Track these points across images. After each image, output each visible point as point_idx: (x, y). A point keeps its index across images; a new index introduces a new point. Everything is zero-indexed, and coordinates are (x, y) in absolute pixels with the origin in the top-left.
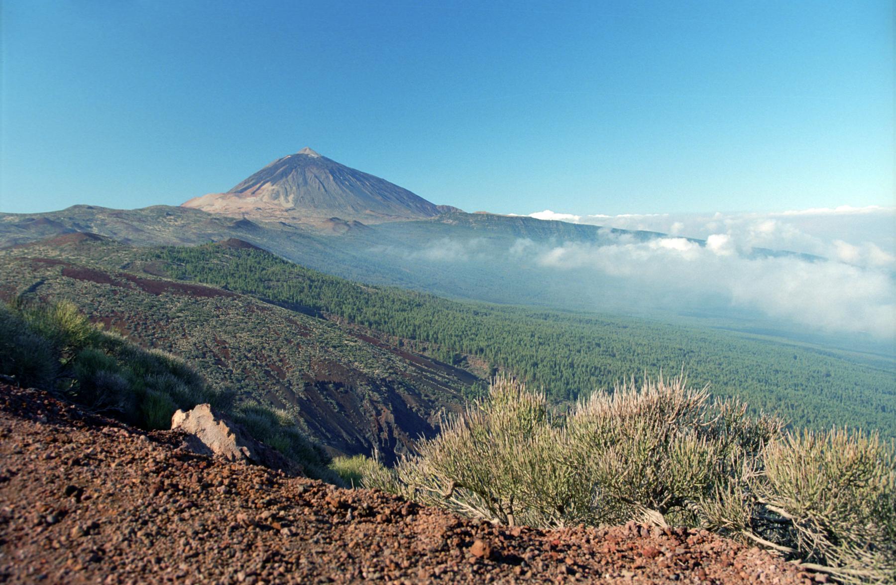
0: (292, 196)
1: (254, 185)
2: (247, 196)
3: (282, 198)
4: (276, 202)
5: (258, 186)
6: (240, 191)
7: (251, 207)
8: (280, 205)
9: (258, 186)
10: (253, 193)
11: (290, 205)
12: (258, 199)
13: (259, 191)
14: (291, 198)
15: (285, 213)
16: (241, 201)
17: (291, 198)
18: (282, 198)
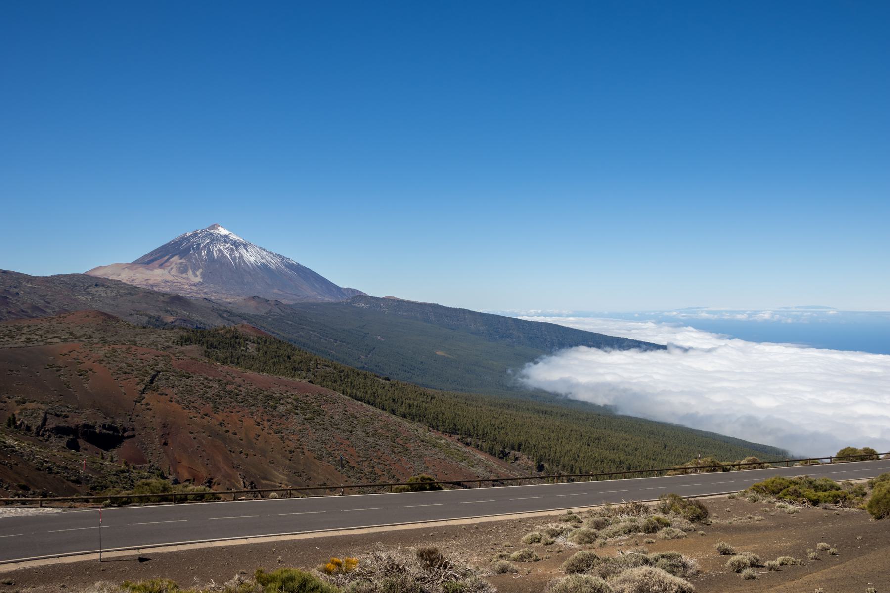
0: (201, 270)
1: (162, 257)
2: (154, 268)
3: (190, 272)
4: (184, 275)
5: (166, 258)
6: (149, 261)
7: (159, 279)
8: (188, 279)
9: (166, 258)
10: (161, 266)
11: (199, 279)
12: (166, 271)
13: (168, 264)
14: (198, 273)
15: (193, 287)
16: (148, 272)
17: (198, 273)
18: (190, 272)
